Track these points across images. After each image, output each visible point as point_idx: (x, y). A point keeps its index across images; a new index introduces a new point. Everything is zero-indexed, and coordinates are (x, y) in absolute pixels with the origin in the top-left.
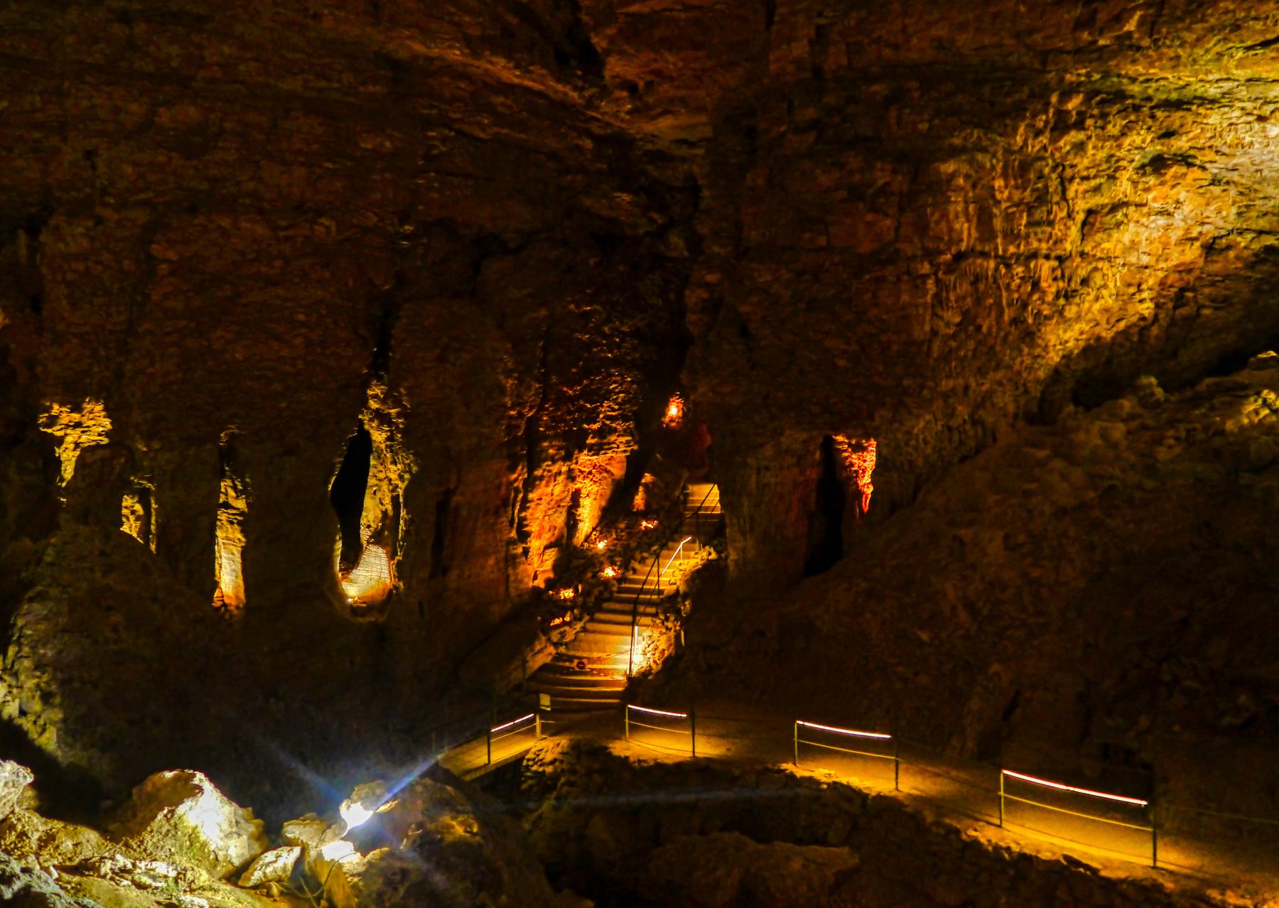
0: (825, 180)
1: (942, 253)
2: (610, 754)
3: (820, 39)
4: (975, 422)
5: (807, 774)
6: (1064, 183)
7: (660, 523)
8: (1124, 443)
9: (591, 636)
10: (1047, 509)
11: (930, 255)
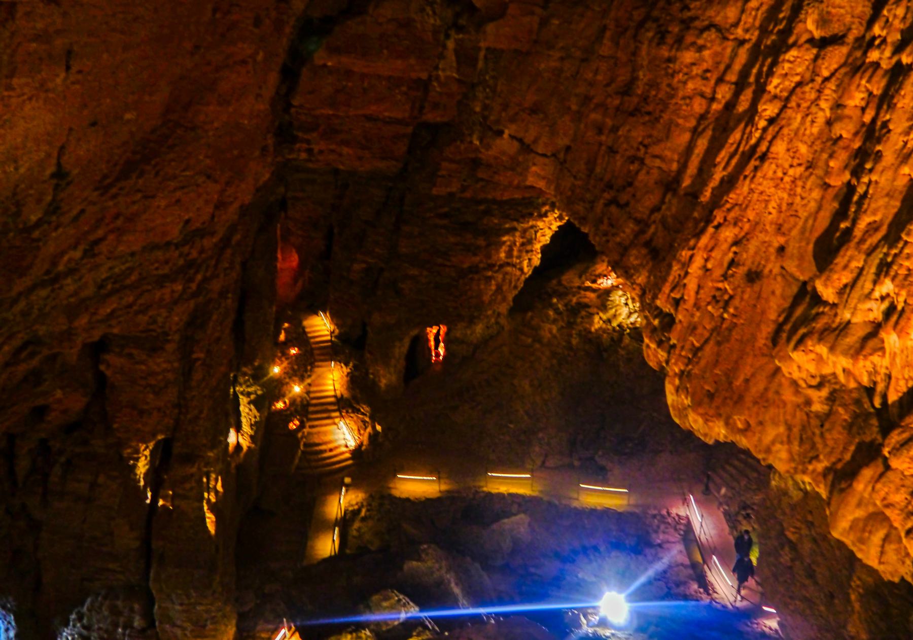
0: (452, 239)
1: (494, 265)
2: (395, 498)
3: (464, 189)
4: (497, 323)
5: (496, 491)
6: (536, 232)
7: (299, 349)
9: (314, 430)
11: (491, 267)
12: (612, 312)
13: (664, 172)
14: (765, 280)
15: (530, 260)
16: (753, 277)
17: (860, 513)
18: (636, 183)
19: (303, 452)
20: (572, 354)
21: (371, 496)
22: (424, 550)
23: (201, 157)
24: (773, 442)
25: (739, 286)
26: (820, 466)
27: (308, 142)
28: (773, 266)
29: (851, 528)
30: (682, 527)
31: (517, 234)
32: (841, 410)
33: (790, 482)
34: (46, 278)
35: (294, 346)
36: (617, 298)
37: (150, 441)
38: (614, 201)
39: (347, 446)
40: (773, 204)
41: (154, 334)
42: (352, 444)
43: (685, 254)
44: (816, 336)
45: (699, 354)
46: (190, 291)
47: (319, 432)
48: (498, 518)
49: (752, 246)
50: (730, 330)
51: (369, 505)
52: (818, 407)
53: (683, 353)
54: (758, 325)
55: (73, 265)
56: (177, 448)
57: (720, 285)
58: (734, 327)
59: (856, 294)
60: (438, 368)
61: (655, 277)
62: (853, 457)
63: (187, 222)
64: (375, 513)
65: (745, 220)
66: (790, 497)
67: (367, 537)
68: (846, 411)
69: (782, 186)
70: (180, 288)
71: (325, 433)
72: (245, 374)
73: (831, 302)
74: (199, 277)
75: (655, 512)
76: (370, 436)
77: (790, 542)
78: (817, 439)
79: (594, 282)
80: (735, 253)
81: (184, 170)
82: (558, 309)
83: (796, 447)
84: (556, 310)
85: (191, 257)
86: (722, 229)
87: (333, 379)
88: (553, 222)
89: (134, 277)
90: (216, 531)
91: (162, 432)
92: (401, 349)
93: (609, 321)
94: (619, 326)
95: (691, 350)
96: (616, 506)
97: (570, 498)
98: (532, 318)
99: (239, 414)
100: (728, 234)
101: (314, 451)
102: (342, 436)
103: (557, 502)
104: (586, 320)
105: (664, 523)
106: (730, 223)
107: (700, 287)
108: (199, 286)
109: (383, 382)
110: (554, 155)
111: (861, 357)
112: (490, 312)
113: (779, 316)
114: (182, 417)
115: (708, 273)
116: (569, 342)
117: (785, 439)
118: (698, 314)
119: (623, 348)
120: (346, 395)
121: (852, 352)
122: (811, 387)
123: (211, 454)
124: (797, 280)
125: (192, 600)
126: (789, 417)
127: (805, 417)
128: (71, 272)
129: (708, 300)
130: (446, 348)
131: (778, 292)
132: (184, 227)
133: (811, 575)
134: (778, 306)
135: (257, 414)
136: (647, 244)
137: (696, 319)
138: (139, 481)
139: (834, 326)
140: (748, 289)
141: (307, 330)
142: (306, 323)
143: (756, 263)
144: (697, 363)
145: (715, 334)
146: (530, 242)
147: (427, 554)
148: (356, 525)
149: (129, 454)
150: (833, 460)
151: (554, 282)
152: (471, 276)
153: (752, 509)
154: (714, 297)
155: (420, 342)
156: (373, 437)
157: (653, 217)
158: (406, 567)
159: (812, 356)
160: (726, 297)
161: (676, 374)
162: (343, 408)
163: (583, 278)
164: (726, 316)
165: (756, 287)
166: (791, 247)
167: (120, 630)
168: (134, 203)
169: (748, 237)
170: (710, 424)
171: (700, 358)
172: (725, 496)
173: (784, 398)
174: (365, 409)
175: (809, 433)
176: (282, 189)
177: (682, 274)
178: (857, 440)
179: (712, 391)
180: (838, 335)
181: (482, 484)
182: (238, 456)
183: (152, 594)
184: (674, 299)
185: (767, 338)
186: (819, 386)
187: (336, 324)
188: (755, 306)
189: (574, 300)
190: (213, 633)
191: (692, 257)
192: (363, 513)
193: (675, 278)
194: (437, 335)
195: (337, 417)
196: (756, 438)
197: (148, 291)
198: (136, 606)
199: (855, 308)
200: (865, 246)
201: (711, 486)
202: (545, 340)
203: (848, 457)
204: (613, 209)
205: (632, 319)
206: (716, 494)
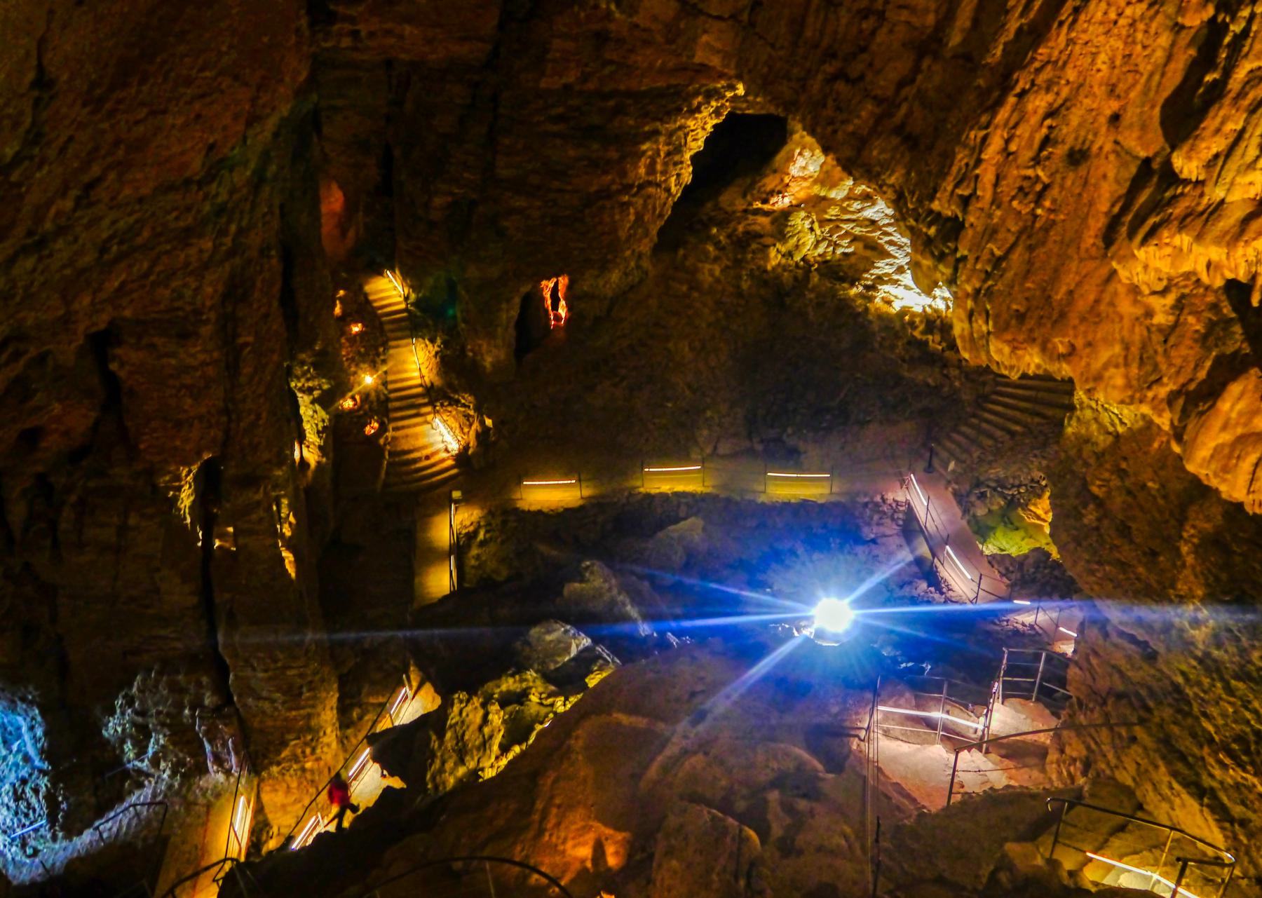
0: (572, 153)
1: (631, 186)
2: (523, 511)
3: (585, 78)
4: (638, 267)
6: (686, 135)
7: (364, 326)
8: (722, 278)
10: (704, 325)
11: (627, 188)
12: (793, 241)
13: (916, 29)
14: (1095, 162)
15: (678, 175)
16: (1077, 157)
17: (1226, 437)
18: (874, 47)
19: (389, 464)
20: (742, 302)
21: (491, 513)
22: (588, 567)
23: (224, 49)
24: (1106, 367)
25: (1057, 171)
26: (1163, 392)
27: (352, 20)
28: (1103, 141)
29: (1212, 456)
30: (901, 516)
31: (662, 139)
32: (1191, 319)
33: (1094, 427)
34: (29, 241)
35: (356, 322)
36: (799, 221)
37: (193, 464)
38: (840, 75)
39: (447, 450)
40: (1103, 57)
41: (180, 313)
42: (454, 447)
43: (975, 135)
44: (1176, 223)
45: (1004, 265)
46: (224, 248)
47: (407, 436)
48: (661, 525)
49: (1075, 117)
50: (1047, 229)
51: (489, 524)
52: (1161, 319)
53: (979, 266)
54: (1085, 220)
55: (63, 222)
56: (230, 470)
57: (1030, 172)
58: (1051, 226)
59: (1234, 164)
60: (561, 335)
61: (919, 173)
62: (1209, 374)
63: (211, 148)
64: (497, 533)
65: (1063, 82)
66: (1097, 444)
67: (492, 565)
68: (1198, 320)
69: (1116, 31)
70: (210, 244)
71: (416, 436)
72: (303, 363)
73: (1194, 179)
74: (233, 228)
75: (867, 500)
76: (478, 435)
77: (1095, 497)
78: (1160, 359)
79: (765, 201)
80: (1050, 127)
81: (202, 70)
82: (720, 242)
83: (1134, 370)
84: (717, 244)
85: (220, 200)
86: (1031, 97)
87: (416, 362)
88: (708, 119)
89: (146, 234)
90: (297, 573)
91: (208, 449)
92: (510, 313)
93: (790, 254)
94: (803, 259)
95: (989, 261)
96: (814, 495)
97: (754, 492)
98: (685, 257)
99: (299, 420)
100: (1039, 103)
101: (403, 463)
102: (440, 439)
103: (738, 498)
104: (759, 256)
105: (879, 512)
106: (1040, 88)
107: (998, 179)
108: (233, 240)
109: (488, 361)
110: (732, 17)
111: (1242, 244)
112: (628, 253)
113: (1113, 206)
114: (233, 425)
115: (1011, 158)
116: (739, 287)
117: (1121, 360)
118: (998, 213)
119: (812, 290)
120: (438, 382)
121: (1228, 238)
122: (1154, 293)
123: (279, 473)
124: (1136, 157)
125: (279, 664)
126: (1125, 333)
127: (1145, 333)
128: (61, 231)
129: (1013, 193)
130: (570, 307)
131: (1111, 175)
132: (207, 155)
133: (1124, 531)
134: (1112, 193)
135: (326, 417)
136: (899, 130)
137: (995, 220)
138: (185, 519)
139: (1201, 208)
140: (1071, 175)
141: (371, 298)
142: (367, 288)
143: (1080, 140)
144: (1001, 276)
145: (1024, 237)
146: (678, 150)
147: (592, 573)
148: (474, 551)
149: (166, 482)
150: (1182, 380)
151: (709, 205)
152: (600, 203)
153: (988, 486)
154: (1021, 189)
155: (532, 301)
156: (482, 436)
157: (904, 93)
158: (566, 592)
159: (1168, 250)
160: (1038, 187)
161: (968, 295)
162: (437, 400)
163: (749, 198)
164: (1039, 211)
165: (1082, 171)
166: (1129, 114)
167: (187, 712)
168: (137, 123)
169: (1068, 104)
170: (1020, 352)
171: (1005, 270)
172: (953, 471)
173: (1119, 309)
174: (468, 399)
175: (1151, 352)
176: (315, 97)
177: (972, 163)
178: (1214, 354)
179: (1022, 310)
180: (1207, 220)
181: (639, 483)
182: (305, 476)
183: (224, 662)
184: (961, 196)
185: (1096, 236)
186: (1164, 292)
187: (411, 287)
188: (1080, 195)
189: (741, 228)
190: (311, 702)
191: (985, 139)
192: (481, 536)
193: (960, 169)
194: (555, 291)
195: (429, 413)
196: (1083, 363)
197: (167, 252)
198: (205, 680)
199: (1232, 183)
200: (1246, 103)
201: (936, 463)
202: (706, 286)
203: (1202, 375)
204: (840, 86)
205: (821, 250)
206: (941, 470)
